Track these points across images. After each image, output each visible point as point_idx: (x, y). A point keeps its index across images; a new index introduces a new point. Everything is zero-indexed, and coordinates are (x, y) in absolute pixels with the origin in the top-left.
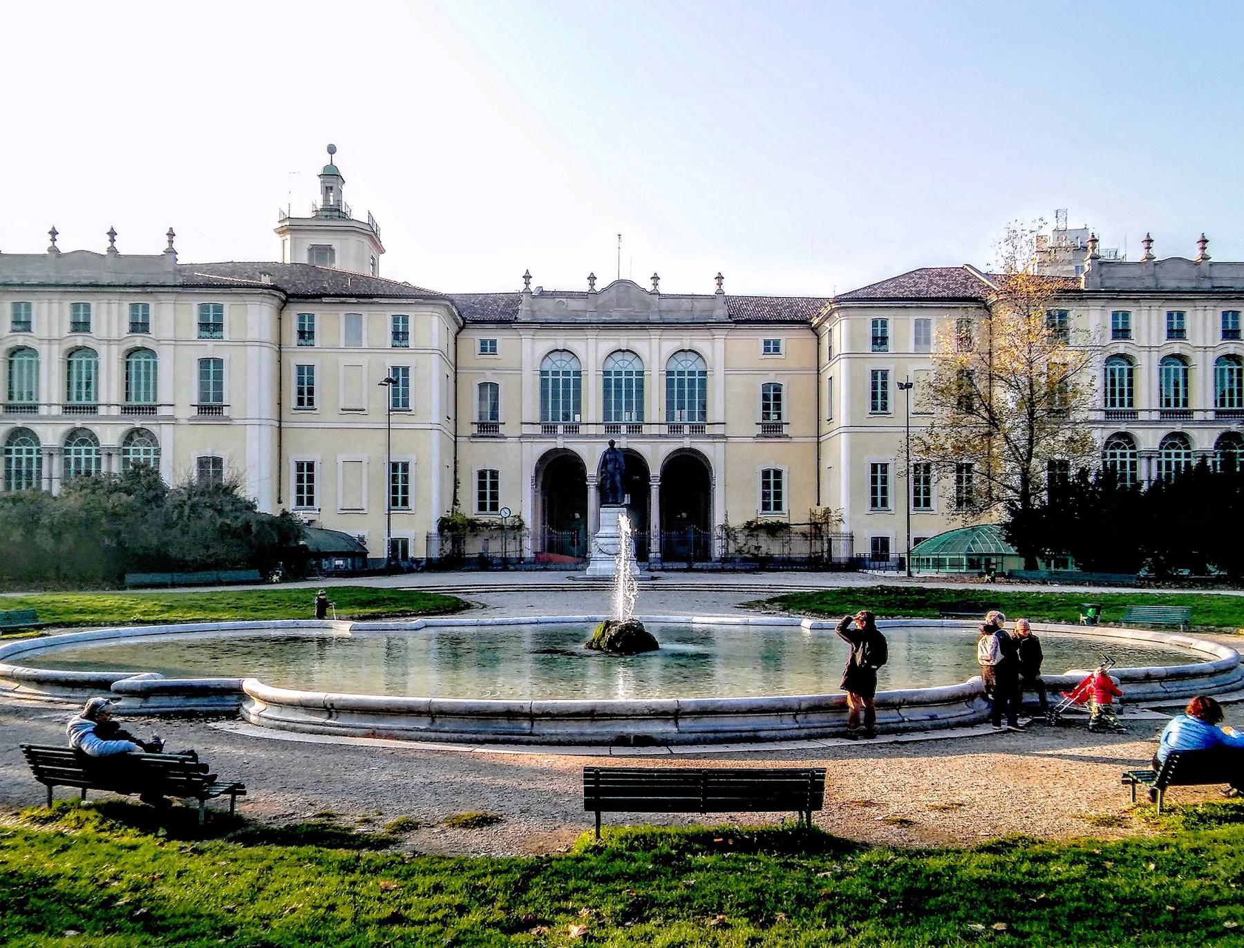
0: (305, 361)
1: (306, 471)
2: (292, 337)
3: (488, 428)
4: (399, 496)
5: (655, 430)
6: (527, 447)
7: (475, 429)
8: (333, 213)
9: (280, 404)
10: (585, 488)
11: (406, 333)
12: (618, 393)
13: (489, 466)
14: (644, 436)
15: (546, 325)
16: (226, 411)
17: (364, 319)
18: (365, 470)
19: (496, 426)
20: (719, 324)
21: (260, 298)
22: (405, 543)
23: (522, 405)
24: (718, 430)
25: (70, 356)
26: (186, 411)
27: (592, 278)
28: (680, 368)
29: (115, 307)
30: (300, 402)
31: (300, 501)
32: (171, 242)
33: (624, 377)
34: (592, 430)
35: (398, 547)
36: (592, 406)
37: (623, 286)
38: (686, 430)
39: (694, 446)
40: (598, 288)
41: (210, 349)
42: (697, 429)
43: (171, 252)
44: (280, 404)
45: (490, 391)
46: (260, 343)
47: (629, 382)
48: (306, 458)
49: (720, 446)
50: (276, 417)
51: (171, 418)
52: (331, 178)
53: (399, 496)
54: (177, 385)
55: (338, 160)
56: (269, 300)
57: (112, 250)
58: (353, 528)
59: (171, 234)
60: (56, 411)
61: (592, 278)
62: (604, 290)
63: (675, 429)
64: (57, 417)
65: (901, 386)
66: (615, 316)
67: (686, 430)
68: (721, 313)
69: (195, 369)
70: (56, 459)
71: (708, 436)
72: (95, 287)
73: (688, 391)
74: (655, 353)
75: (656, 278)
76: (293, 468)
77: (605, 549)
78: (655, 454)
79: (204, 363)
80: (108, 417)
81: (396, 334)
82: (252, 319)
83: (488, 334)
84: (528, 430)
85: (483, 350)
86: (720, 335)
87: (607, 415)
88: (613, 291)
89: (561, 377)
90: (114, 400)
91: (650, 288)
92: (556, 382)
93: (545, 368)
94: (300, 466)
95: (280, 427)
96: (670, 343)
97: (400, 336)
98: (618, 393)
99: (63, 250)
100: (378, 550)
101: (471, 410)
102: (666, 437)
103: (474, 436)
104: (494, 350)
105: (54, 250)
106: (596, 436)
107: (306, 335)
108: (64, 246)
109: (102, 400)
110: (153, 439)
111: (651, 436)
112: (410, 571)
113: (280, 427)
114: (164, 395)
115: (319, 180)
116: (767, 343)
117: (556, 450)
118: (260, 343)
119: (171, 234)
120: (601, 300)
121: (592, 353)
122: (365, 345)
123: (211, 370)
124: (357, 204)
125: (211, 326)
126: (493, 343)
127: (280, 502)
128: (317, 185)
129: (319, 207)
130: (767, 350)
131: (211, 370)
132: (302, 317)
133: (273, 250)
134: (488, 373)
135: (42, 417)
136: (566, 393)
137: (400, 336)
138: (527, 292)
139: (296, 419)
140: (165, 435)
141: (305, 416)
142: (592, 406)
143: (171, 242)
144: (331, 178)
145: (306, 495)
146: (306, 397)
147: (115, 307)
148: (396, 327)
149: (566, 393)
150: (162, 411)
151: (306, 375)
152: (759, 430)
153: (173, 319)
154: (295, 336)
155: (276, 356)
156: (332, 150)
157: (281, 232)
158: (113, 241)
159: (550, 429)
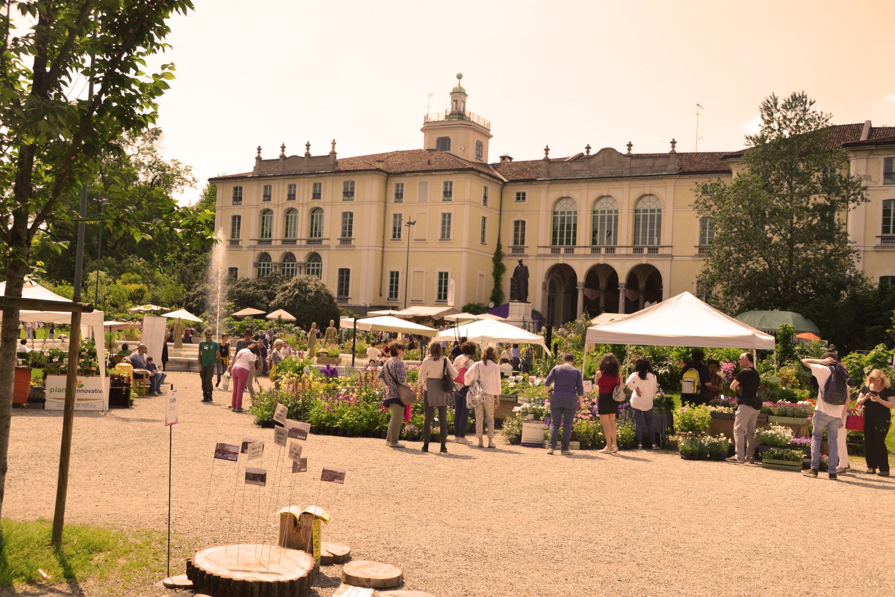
0: (397, 212)
1: (395, 275)
5: (623, 251)
6: (540, 262)
8: (458, 115)
9: (384, 237)
11: (451, 192)
14: (615, 256)
15: (555, 181)
16: (240, 243)
17: (429, 185)
19: (522, 250)
20: (670, 176)
21: (371, 176)
23: (539, 233)
24: (667, 251)
25: (313, 212)
27: (588, 148)
28: (645, 207)
29: (306, 185)
30: (394, 236)
31: (391, 295)
32: (333, 147)
33: (606, 214)
36: (625, 234)
37: (608, 152)
38: (646, 251)
39: (650, 263)
40: (592, 153)
41: (348, 207)
42: (653, 250)
43: (333, 153)
44: (384, 237)
45: (520, 226)
46: (371, 202)
47: (652, 217)
48: (395, 269)
49: (667, 263)
50: (381, 245)
51: (328, 246)
52: (458, 94)
54: (331, 229)
55: (464, 84)
56: (376, 176)
57: (308, 155)
59: (334, 143)
61: (588, 148)
62: (595, 155)
63: (638, 250)
64: (279, 247)
65: (409, 223)
66: (601, 173)
67: (646, 251)
68: (672, 167)
70: (303, 269)
72: (297, 175)
73: (648, 224)
74: (624, 198)
75: (630, 145)
80: (300, 246)
82: (369, 189)
83: (521, 189)
84: (542, 251)
85: (518, 199)
86: (670, 182)
87: (635, 241)
88: (601, 156)
89: (606, 214)
90: (304, 237)
91: (624, 151)
92: (645, 217)
93: (638, 207)
94: (392, 273)
95: (383, 251)
96: (636, 189)
97: (448, 194)
98: (645, 226)
99: (287, 156)
102: (588, 255)
104: (524, 199)
105: (308, 155)
106: (585, 255)
107: (399, 196)
108: (314, 153)
109: (299, 237)
113: (383, 251)
114: (325, 235)
115: (450, 96)
118: (371, 202)
119: (334, 143)
120: (592, 162)
121: (583, 200)
122: (428, 200)
123: (348, 218)
124: (474, 109)
125: (349, 194)
126: (524, 194)
127: (381, 295)
128: (449, 99)
129: (449, 111)
131: (348, 218)
132: (398, 185)
133: (416, 142)
134: (520, 214)
135: (274, 247)
136: (652, 225)
137: (448, 194)
138: (546, 160)
139: (393, 247)
140: (324, 255)
141: (396, 244)
142: (625, 234)
143: (333, 147)
144: (458, 94)
146: (397, 234)
147: (306, 185)
148: (446, 189)
149: (652, 225)
150: (324, 243)
152: (696, 251)
153: (332, 189)
155: (382, 209)
156: (459, 77)
157: (423, 130)
158: (308, 149)
159: (556, 251)
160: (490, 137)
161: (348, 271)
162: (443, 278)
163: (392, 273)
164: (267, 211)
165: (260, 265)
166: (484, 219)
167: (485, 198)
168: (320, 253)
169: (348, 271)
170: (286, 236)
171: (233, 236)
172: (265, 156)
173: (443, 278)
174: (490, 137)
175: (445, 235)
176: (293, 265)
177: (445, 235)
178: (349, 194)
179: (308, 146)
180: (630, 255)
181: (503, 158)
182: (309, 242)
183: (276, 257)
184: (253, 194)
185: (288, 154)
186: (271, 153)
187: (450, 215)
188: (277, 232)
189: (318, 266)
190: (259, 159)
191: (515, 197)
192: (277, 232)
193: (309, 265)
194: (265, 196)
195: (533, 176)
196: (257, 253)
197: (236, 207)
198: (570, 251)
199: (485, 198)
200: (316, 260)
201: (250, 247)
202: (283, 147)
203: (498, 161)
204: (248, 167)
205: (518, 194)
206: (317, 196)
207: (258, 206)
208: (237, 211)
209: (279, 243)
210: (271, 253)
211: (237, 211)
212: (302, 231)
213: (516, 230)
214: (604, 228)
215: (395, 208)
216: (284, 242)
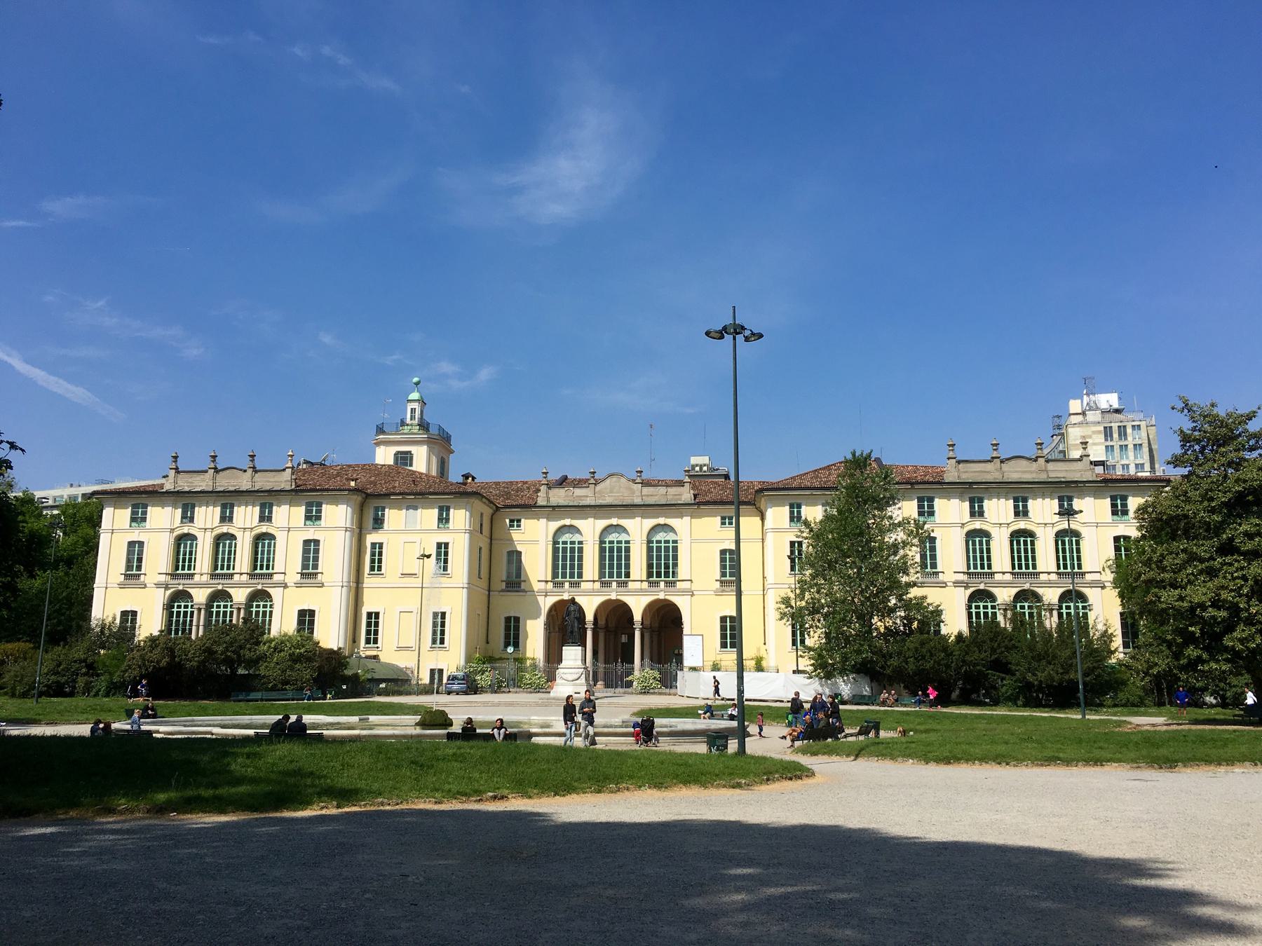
1: (374, 617)
2: (369, 522)
5: (637, 585)
13: (512, 614)
19: (519, 584)
24: (686, 585)
26: (293, 576)
35: (436, 673)
53: (439, 638)
54: (287, 558)
58: (403, 661)
60: (205, 578)
78: (638, 606)
79: (307, 543)
81: (440, 520)
94: (369, 615)
101: (501, 572)
107: (378, 523)
110: (269, 596)
114: (278, 567)
116: (723, 518)
117: (608, 602)
123: (311, 550)
130: (723, 523)
131: (311, 550)
132: (377, 509)
145: (373, 637)
146: (377, 565)
150: (276, 578)
151: (378, 548)
154: (371, 521)
160: (452, 452)
161: (312, 613)
163: (369, 615)
169: (312, 613)
173: (440, 620)
174: (452, 452)
181: (466, 476)
182: (213, 576)
187: (446, 545)
195: (531, 502)
198: (575, 585)
203: (461, 480)
207: (172, 530)
214: (614, 561)
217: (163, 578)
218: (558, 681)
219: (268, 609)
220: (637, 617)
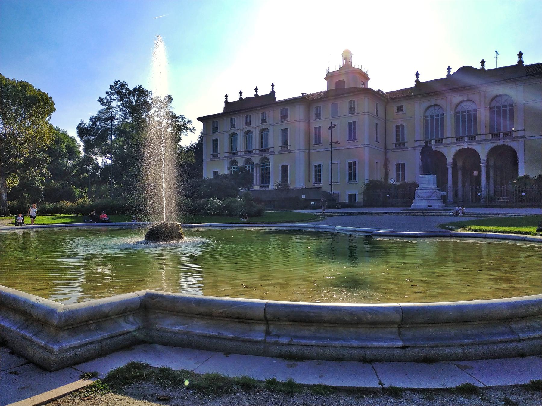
1: (318, 168)
2: (313, 117)
3: (400, 144)
4: (352, 176)
5: (483, 137)
7: (394, 146)
9: (309, 144)
10: (446, 169)
12: (464, 122)
14: (477, 141)
17: (338, 104)
18: (339, 167)
22: (355, 195)
31: (316, 181)
32: (273, 88)
34: (449, 141)
35: (352, 197)
39: (506, 143)
40: (452, 73)
46: (299, 120)
48: (318, 163)
51: (273, 152)
53: (352, 176)
59: (273, 85)
69: (280, 133)
71: (515, 138)
75: (483, 62)
76: (314, 167)
77: (421, 195)
80: (256, 154)
85: (398, 110)
91: (479, 67)
100: (346, 199)
101: (392, 138)
103: (394, 149)
104: (402, 110)
106: (451, 143)
107: (318, 116)
111: (481, 141)
112: (356, 207)
113: (309, 153)
118: (299, 120)
119: (273, 85)
123: (284, 132)
126: (402, 107)
132: (316, 108)
135: (239, 156)
140: (271, 158)
143: (273, 88)
148: (350, 106)
150: (271, 150)
154: (314, 116)
158: (256, 92)
161: (287, 167)
162: (352, 165)
163: (316, 166)
164: (234, 134)
165: (231, 168)
166: (377, 124)
167: (377, 111)
168: (268, 157)
169: (287, 167)
170: (247, 149)
171: (214, 152)
172: (230, 100)
173: (352, 165)
175: (352, 137)
176: (252, 167)
177: (352, 137)
178: (284, 118)
179: (256, 89)
180: (489, 140)
183: (241, 162)
184: (224, 126)
185: (244, 96)
186: (234, 98)
188: (241, 146)
189: (267, 165)
190: (226, 102)
191: (395, 110)
192: (241, 146)
193: (262, 166)
194: (231, 125)
196: (229, 161)
197: (215, 134)
199: (377, 111)
200: (266, 162)
201: (225, 157)
202: (241, 93)
204: (220, 109)
205: (398, 107)
206: (264, 121)
207: (228, 132)
208: (215, 136)
209: (242, 153)
210: (238, 160)
211: (215, 136)
212: (256, 145)
213: (398, 131)
215: (315, 124)
216: (245, 152)
217: (226, 155)
218: (416, 198)
219: (266, 167)
220: (483, 157)
